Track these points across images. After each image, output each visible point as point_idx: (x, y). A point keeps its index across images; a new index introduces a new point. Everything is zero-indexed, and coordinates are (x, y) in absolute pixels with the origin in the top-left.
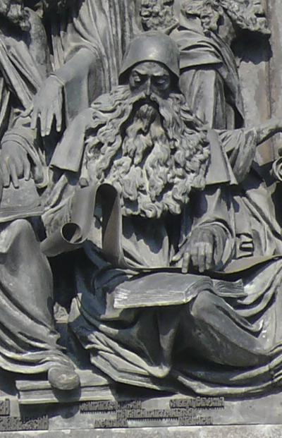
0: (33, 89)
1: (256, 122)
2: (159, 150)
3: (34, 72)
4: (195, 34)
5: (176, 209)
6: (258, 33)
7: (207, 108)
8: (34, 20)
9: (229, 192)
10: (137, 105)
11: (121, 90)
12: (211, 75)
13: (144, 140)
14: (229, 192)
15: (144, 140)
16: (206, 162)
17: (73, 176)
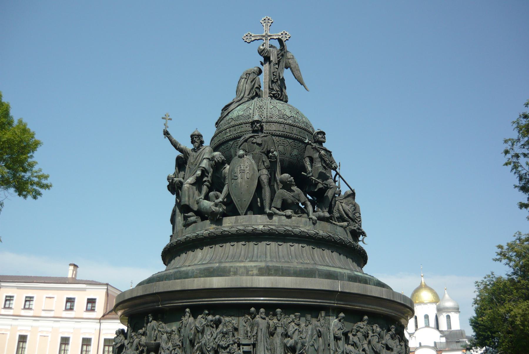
0: (214, 333)
1: (236, 337)
2: (225, 340)
3: (214, 331)
4: (230, 328)
5: (227, 346)
6: (237, 328)
7: (231, 335)
8: (215, 326)
9: (232, 344)
10: (223, 336)
11: (222, 334)
12: (232, 332)
13: (224, 339)
14: (232, 344)
15: (224, 339)
16: (230, 341)
17: (217, 342)
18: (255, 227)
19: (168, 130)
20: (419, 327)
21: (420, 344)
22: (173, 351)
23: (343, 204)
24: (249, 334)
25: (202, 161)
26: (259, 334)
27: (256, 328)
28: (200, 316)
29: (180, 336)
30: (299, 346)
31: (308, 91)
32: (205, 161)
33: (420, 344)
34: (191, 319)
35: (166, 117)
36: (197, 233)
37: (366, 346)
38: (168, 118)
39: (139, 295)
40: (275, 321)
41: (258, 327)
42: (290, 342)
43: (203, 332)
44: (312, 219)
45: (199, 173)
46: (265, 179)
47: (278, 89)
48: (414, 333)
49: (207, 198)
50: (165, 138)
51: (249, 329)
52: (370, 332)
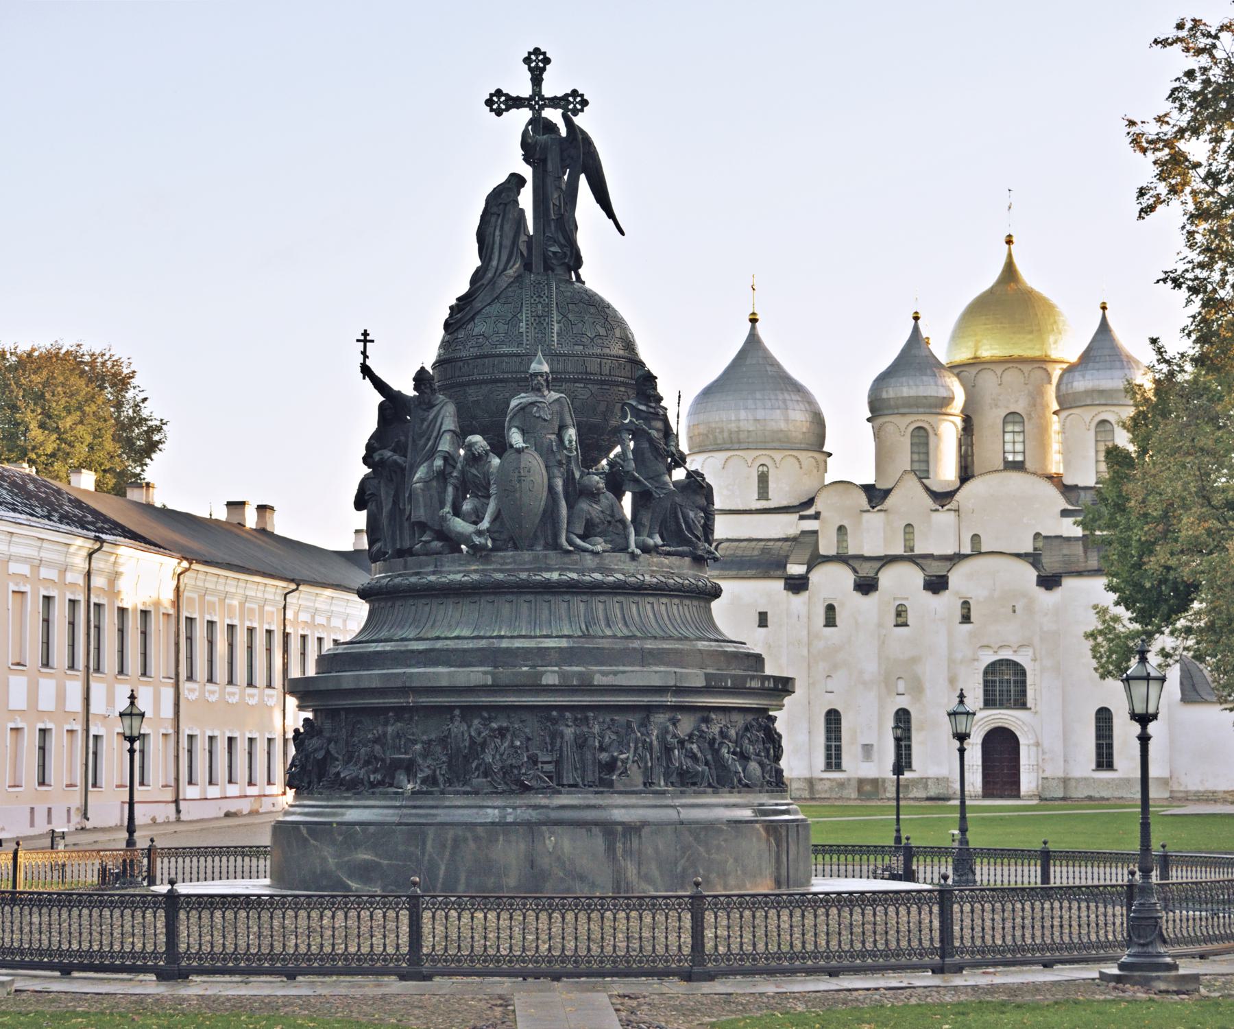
18: (547, 575)
19: (368, 362)
20: (976, 471)
21: (976, 538)
22: (438, 772)
23: (685, 510)
24: (549, 748)
25: (439, 436)
26: (565, 749)
27: (559, 740)
28: (476, 722)
29: (445, 748)
30: (619, 763)
31: (622, 233)
32: (447, 437)
33: (976, 538)
34: (464, 727)
35: (362, 338)
36: (451, 577)
37: (709, 757)
38: (368, 338)
39: (374, 686)
40: (585, 729)
41: (562, 738)
42: (604, 756)
43: (484, 745)
44: (633, 553)
45: (439, 463)
46: (559, 484)
47: (562, 241)
48: (950, 495)
49: (457, 512)
50: (364, 378)
51: (548, 740)
52: (717, 737)
